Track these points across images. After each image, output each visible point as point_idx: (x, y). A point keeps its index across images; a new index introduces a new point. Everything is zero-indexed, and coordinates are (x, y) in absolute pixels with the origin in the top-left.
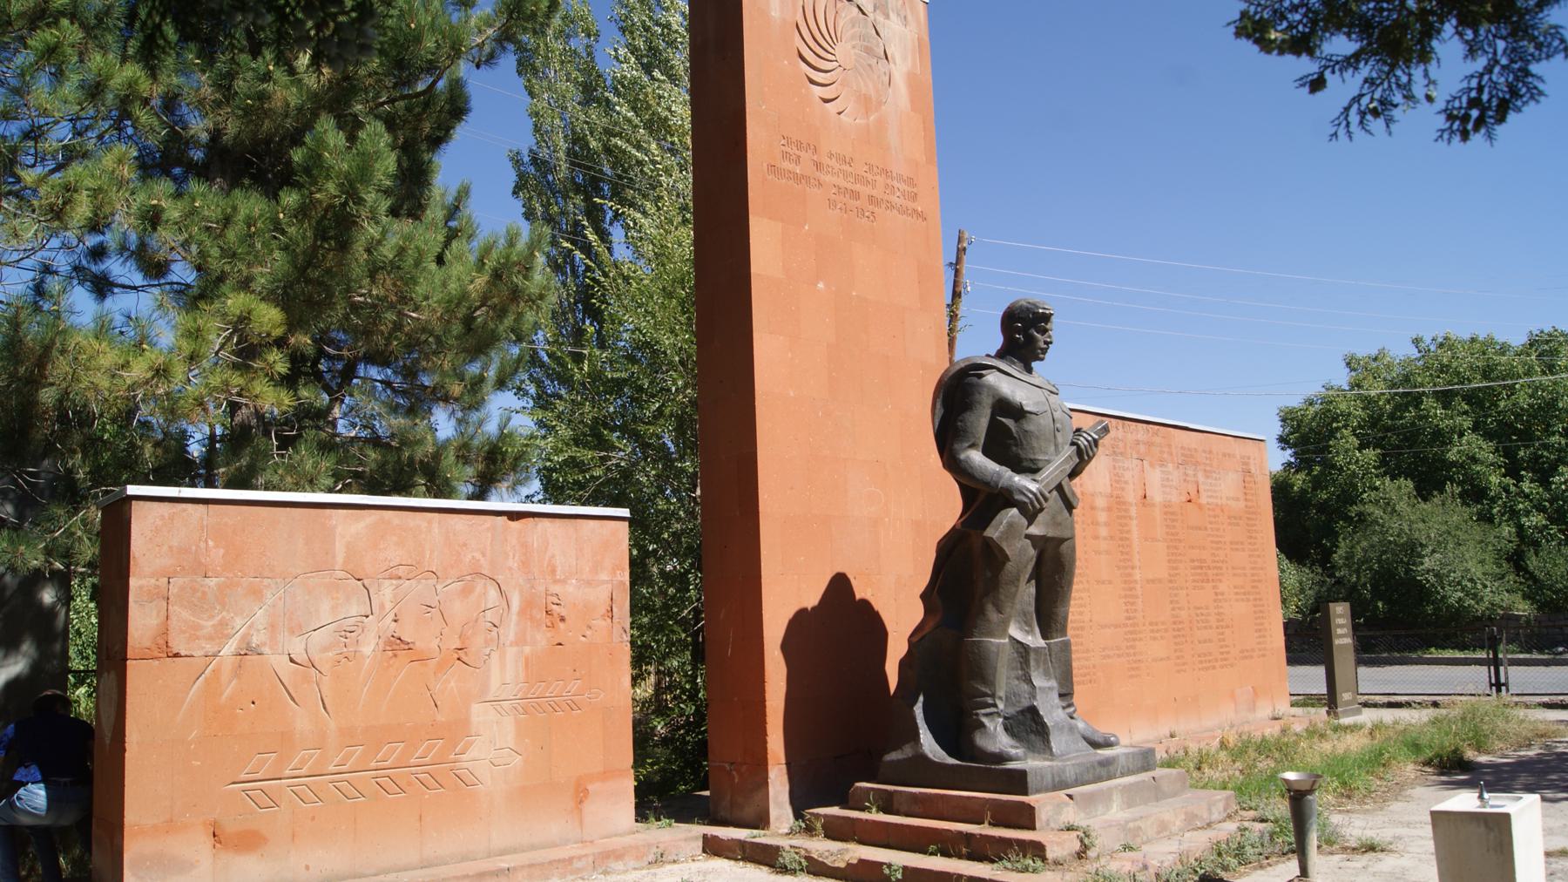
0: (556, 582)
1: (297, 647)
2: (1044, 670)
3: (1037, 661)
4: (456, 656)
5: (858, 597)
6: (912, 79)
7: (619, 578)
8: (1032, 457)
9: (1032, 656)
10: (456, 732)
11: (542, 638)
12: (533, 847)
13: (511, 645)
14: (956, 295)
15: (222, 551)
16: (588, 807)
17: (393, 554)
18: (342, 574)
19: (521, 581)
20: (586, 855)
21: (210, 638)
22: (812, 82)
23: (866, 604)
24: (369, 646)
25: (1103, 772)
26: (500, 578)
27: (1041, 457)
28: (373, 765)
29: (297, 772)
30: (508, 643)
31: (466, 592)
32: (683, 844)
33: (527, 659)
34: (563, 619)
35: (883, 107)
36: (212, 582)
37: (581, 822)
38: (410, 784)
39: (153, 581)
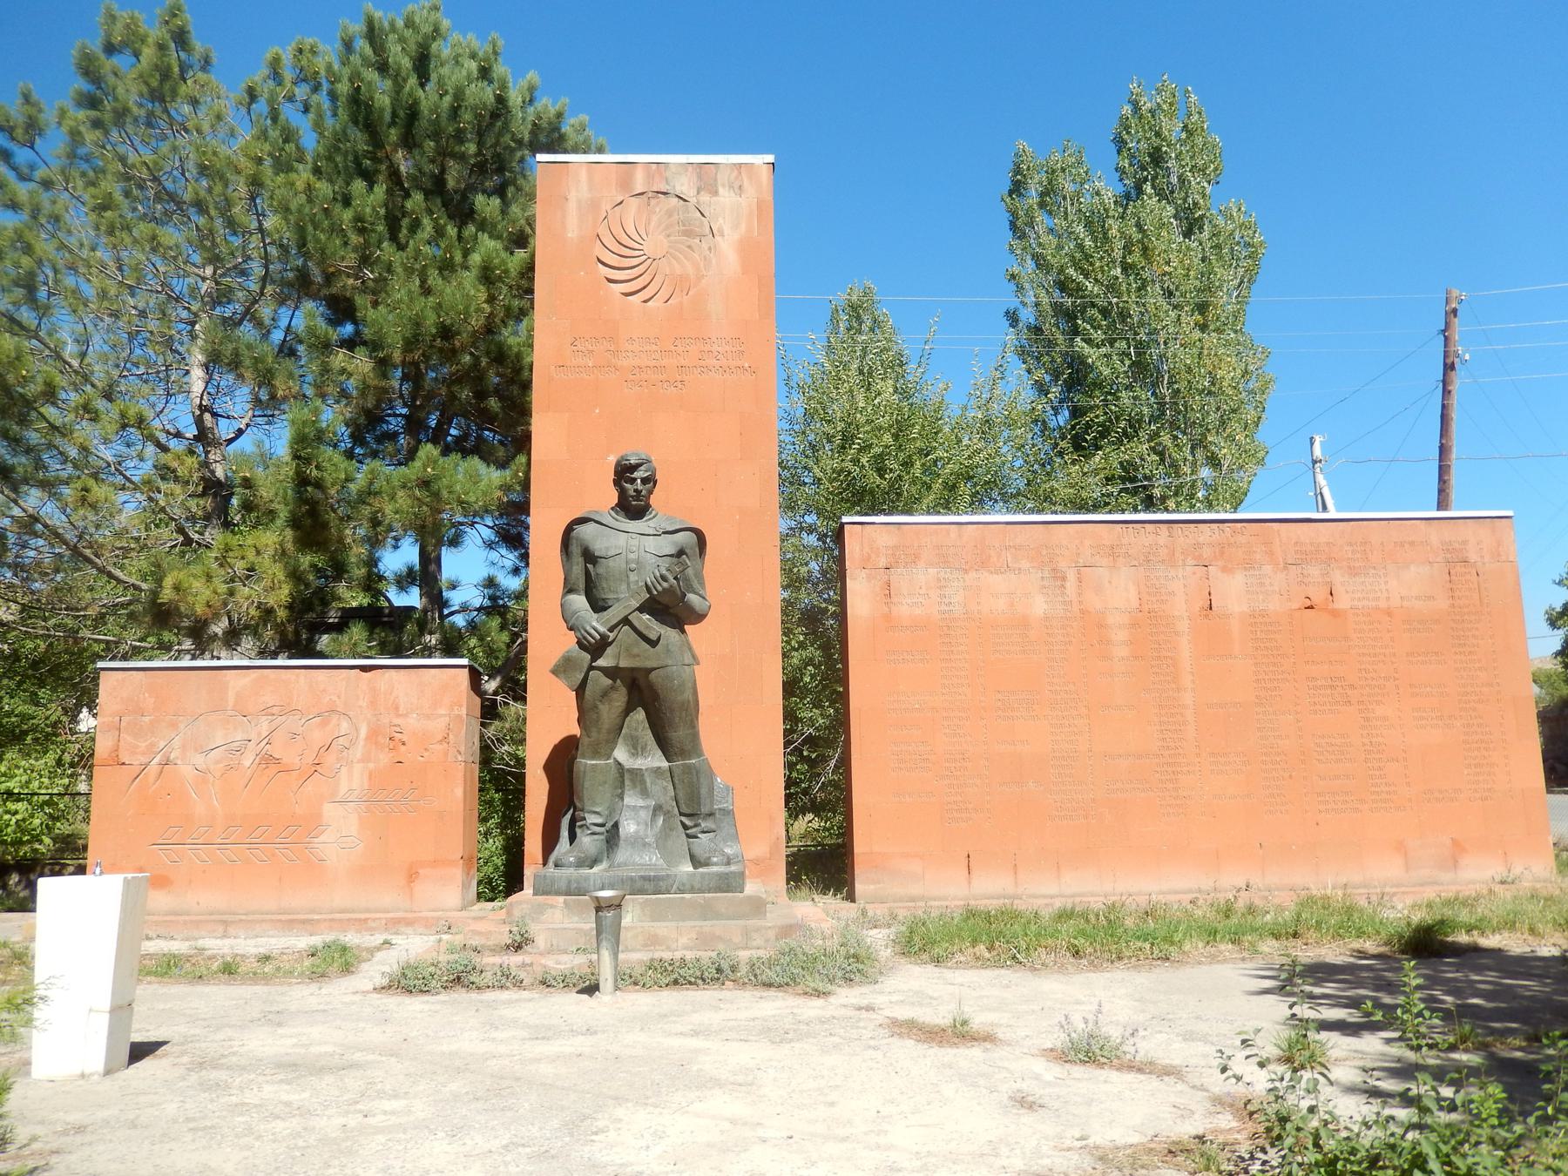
0: (399, 716)
1: (199, 760)
3: (632, 780)
4: (314, 769)
6: (746, 248)
7: (457, 712)
8: (604, 597)
9: (627, 776)
10: (312, 824)
11: (384, 758)
12: (368, 910)
13: (358, 762)
14: (1449, 367)
15: (153, 700)
17: (269, 699)
18: (234, 713)
20: (380, 919)
21: (144, 754)
24: (248, 760)
25: (647, 886)
26: (351, 714)
28: (248, 840)
29: (195, 841)
31: (325, 723)
32: (470, 921)
34: (404, 744)
36: (147, 719)
38: (273, 855)
39: (111, 719)
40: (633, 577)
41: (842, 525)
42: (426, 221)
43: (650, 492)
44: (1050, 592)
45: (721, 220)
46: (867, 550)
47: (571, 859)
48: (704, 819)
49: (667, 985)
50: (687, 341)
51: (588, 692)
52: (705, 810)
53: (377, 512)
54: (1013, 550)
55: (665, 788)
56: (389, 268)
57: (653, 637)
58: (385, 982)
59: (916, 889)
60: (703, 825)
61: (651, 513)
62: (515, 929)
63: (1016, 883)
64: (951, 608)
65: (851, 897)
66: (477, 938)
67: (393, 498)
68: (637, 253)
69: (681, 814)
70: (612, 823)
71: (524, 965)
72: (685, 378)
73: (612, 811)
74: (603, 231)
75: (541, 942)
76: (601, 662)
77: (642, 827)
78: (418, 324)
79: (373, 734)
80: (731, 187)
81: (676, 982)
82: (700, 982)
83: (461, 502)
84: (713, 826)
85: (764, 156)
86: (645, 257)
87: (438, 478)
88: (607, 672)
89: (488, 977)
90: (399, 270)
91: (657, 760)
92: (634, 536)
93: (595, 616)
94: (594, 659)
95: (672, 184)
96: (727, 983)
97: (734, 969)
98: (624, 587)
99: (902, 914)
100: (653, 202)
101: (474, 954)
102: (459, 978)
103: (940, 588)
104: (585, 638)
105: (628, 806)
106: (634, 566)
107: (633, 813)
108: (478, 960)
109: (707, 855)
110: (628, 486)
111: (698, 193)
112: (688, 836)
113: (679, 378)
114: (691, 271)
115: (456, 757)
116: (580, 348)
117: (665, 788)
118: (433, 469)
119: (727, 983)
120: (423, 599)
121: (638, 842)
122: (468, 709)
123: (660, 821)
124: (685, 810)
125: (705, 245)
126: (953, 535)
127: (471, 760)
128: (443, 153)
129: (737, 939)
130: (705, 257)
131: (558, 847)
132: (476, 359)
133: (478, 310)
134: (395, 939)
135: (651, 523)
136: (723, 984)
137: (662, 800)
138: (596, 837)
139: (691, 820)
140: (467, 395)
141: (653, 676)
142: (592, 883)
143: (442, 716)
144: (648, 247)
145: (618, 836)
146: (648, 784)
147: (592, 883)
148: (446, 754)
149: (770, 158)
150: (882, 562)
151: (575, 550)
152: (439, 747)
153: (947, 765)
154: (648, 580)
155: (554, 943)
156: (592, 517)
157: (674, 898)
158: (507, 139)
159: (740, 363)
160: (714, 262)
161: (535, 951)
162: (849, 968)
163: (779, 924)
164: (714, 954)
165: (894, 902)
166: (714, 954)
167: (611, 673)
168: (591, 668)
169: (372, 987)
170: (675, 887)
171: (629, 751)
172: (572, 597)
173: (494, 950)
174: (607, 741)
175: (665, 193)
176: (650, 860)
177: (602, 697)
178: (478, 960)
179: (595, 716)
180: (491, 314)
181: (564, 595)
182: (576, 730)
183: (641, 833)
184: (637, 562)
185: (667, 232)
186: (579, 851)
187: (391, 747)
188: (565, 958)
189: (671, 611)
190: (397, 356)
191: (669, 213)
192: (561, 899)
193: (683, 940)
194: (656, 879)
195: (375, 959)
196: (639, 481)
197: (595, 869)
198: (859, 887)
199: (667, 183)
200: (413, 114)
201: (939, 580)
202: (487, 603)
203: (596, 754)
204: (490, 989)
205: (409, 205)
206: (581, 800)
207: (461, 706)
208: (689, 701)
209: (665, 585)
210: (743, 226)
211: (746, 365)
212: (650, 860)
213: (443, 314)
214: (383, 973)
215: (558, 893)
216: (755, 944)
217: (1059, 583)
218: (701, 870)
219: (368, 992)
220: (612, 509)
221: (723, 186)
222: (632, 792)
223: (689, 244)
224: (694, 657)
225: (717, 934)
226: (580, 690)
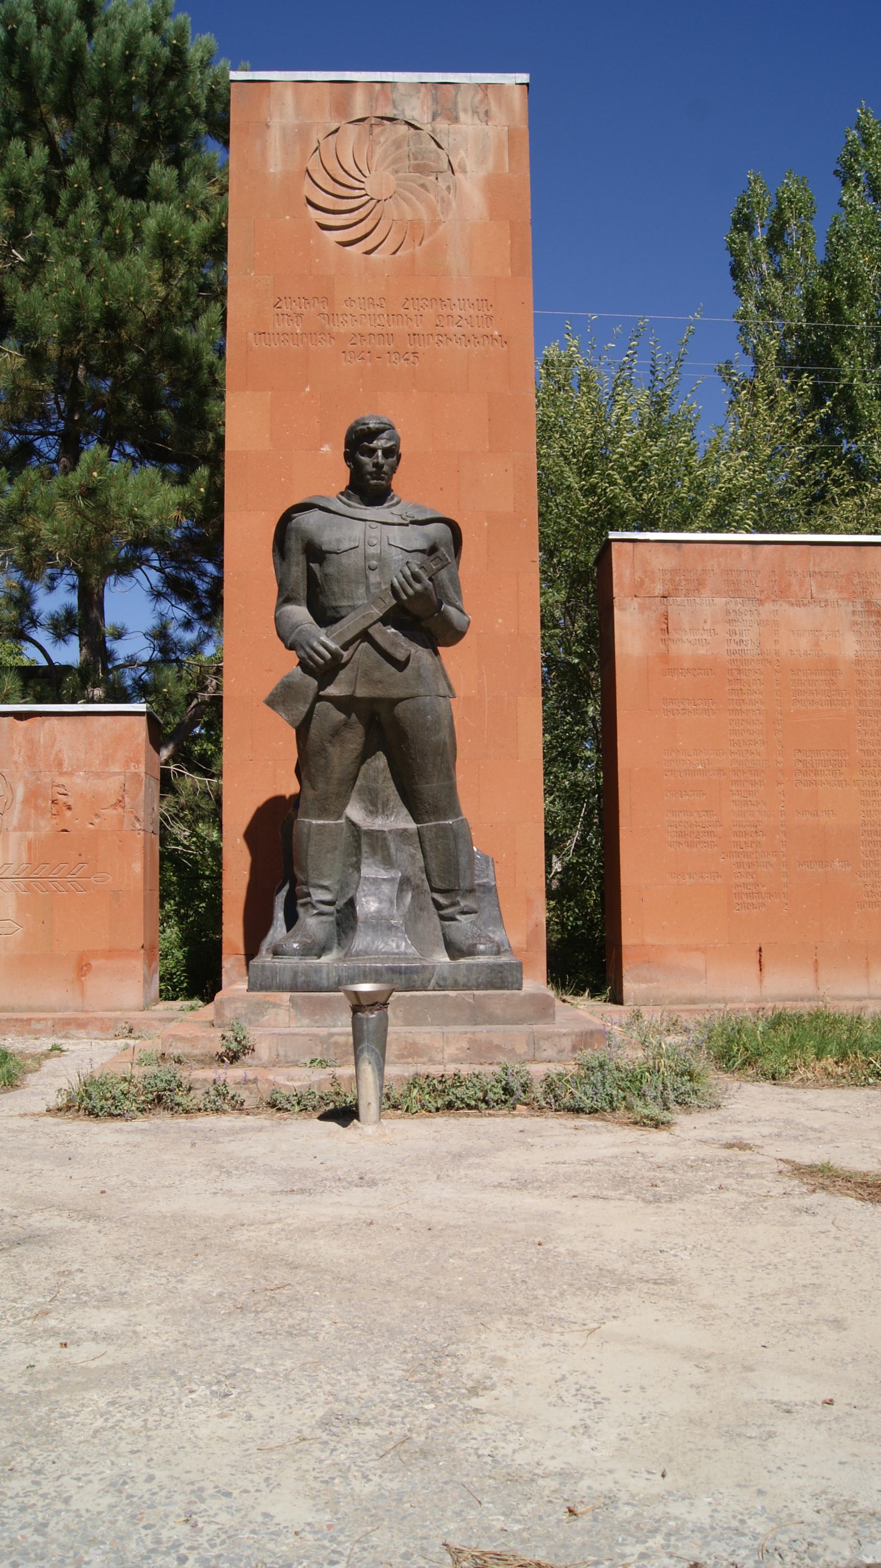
0: (62, 774)
2: (384, 858)
7: (133, 770)
8: (334, 604)
9: (364, 840)
11: (46, 826)
12: (31, 1009)
13: (15, 830)
16: (90, 981)
19: (26, 774)
20: (45, 1019)
22: (324, 227)
27: (345, 603)
30: (11, 828)
32: (156, 1023)
33: (30, 844)
35: (441, 228)
37: (83, 994)
40: (374, 578)
41: (609, 542)
42: (91, 194)
43: (393, 470)
44: (863, 630)
45: (462, 153)
46: (639, 574)
47: (295, 945)
48: (463, 897)
49: (437, 1109)
50: (421, 302)
51: (314, 731)
52: (464, 884)
53: (32, 535)
54: (819, 578)
55: (413, 856)
56: (45, 248)
57: (400, 656)
58: (62, 1101)
59: (697, 989)
60: (462, 904)
61: (392, 499)
62: (229, 1034)
63: (817, 981)
64: (743, 647)
65: (617, 999)
66: (179, 1045)
67: (49, 515)
68: (357, 193)
69: (433, 890)
70: (345, 900)
71: (246, 1081)
72: (419, 349)
73: (344, 885)
74: (313, 164)
75: (263, 1051)
76: (332, 690)
77: (385, 905)
78: (78, 306)
79: (32, 797)
80: (475, 112)
81: (450, 1106)
82: (483, 1106)
83: (133, 516)
84: (474, 906)
85: (517, 75)
86: (367, 198)
87: (105, 485)
88: (338, 702)
89: (197, 1098)
90: (56, 249)
91: (403, 821)
92: (374, 525)
93: (323, 631)
94: (322, 687)
95: (400, 108)
96: (518, 1106)
97: (525, 1088)
98: (362, 590)
99: (688, 1020)
100: (377, 130)
101: (170, 1065)
102: (159, 1098)
103: (730, 622)
104: (311, 658)
105: (366, 879)
106: (374, 563)
107: (373, 888)
108: (185, 1074)
109: (470, 942)
110: (365, 459)
111: (434, 119)
112: (443, 918)
113: (411, 349)
114: (424, 215)
115: (133, 825)
116: (285, 310)
117: (413, 856)
118: (100, 473)
119: (518, 1106)
120: (84, 651)
121: (382, 925)
122: (146, 767)
123: (408, 898)
124: (439, 884)
125: (442, 185)
126: (744, 557)
127: (151, 829)
128: (107, 114)
129: (522, 1049)
130: (442, 198)
131: (271, 932)
132: (147, 360)
133: (151, 293)
134: (66, 1044)
135: (394, 510)
136: (514, 1109)
137: (410, 872)
138: (324, 918)
139: (445, 897)
140: (134, 405)
141: (399, 709)
142: (324, 976)
143: (114, 774)
144: (371, 186)
145: (355, 917)
146: (393, 850)
147: (324, 976)
148: (121, 821)
149: (524, 78)
150: (659, 589)
151: (295, 546)
152: (111, 812)
153: (736, 839)
154: (395, 580)
155: (281, 1053)
156: (316, 502)
157: (435, 996)
158: (181, 100)
159: (487, 331)
160: (454, 204)
161: (256, 1062)
162: (683, 1089)
163: (577, 1030)
164: (497, 1069)
165: (670, 1003)
166: (497, 1069)
167: (343, 704)
168: (318, 698)
169: (45, 1108)
170: (433, 982)
171: (366, 809)
172: (290, 608)
173: (204, 1061)
174: (338, 795)
175: (391, 120)
176: (398, 947)
177: (333, 736)
178: (185, 1074)
179: (322, 761)
180: (166, 298)
181: (279, 606)
182: (290, 786)
183: (385, 913)
184: (380, 558)
185: (396, 167)
186: (305, 936)
187: (54, 812)
188: (296, 1071)
189: (423, 624)
190: (53, 351)
191: (398, 145)
192: (286, 996)
193: (451, 1050)
194: (409, 971)
195: (44, 1070)
196: (380, 453)
197: (325, 959)
198: (629, 986)
199: (395, 107)
200: (76, 64)
201: (728, 612)
202: (157, 655)
203: (323, 812)
204: (202, 1113)
205: (71, 171)
206: (304, 870)
207: (138, 762)
208: (445, 743)
209: (418, 586)
210: (491, 162)
211: (496, 333)
212: (398, 947)
213: (109, 297)
214: (60, 1090)
215: (281, 988)
216: (545, 1055)
218: (462, 960)
219: (40, 1115)
220: (342, 493)
221: (465, 110)
222: (370, 861)
223: (422, 181)
224: (450, 686)
225: (496, 1043)
226: (302, 730)
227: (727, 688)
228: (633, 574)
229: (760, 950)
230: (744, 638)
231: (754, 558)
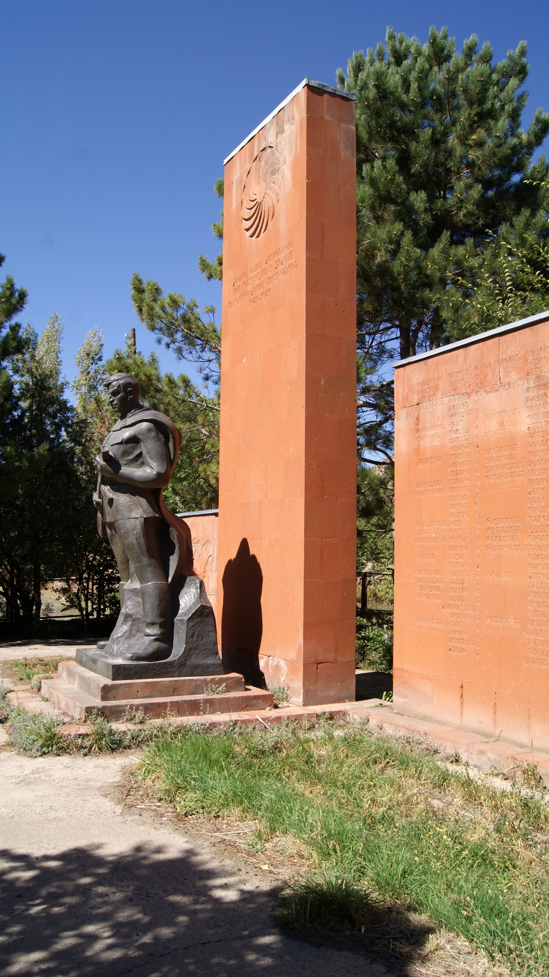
5: (251, 553)
23: (254, 557)
46: (406, 390)
63: (495, 722)
126: (460, 360)
217: (541, 392)
227: (450, 470)
228: (403, 391)
229: (462, 687)
230: (459, 428)
231: (466, 358)
